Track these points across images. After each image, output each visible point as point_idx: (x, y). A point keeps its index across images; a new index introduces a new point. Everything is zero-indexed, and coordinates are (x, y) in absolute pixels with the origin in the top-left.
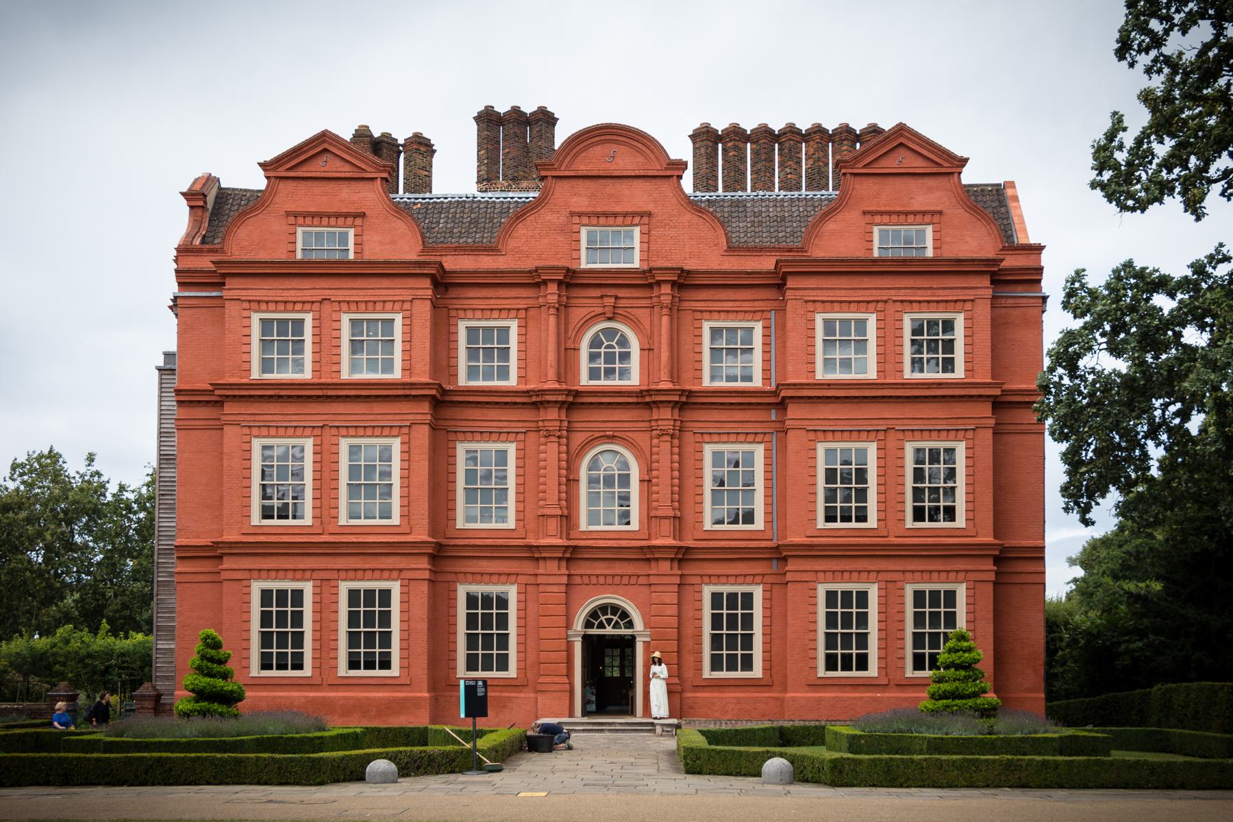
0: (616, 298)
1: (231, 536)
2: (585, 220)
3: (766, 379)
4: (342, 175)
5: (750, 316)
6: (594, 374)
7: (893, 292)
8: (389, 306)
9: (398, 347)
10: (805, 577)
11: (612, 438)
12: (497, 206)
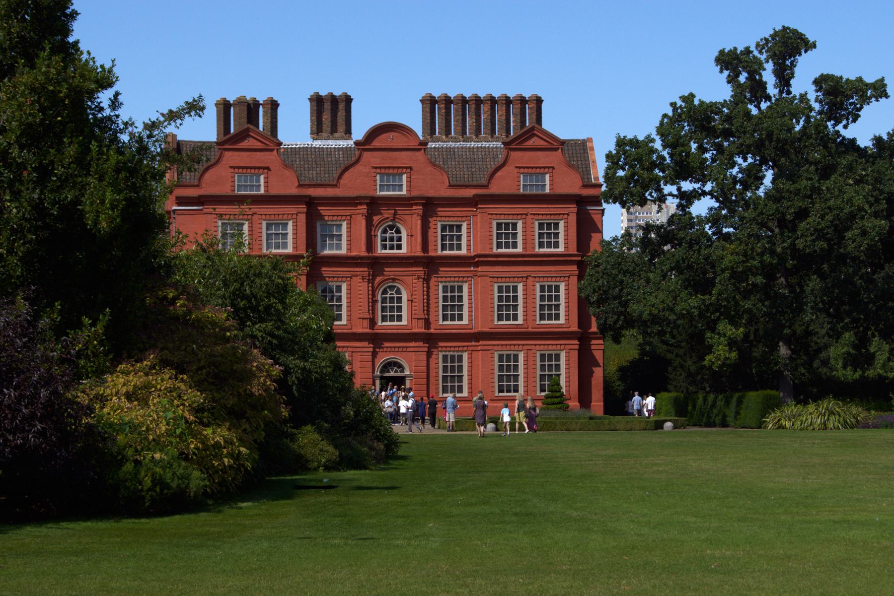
0: (395, 210)
2: (378, 170)
3: (469, 250)
4: (257, 147)
5: (460, 219)
7: (530, 210)
8: (286, 216)
9: (290, 237)
10: (489, 348)
11: (394, 280)
12: (325, 150)
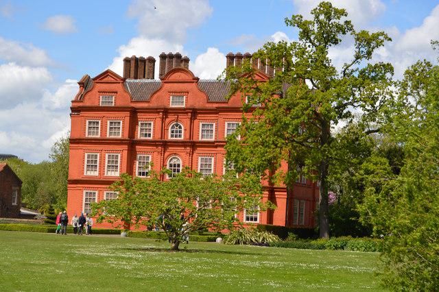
1: (80, 178)
6: (172, 136)
